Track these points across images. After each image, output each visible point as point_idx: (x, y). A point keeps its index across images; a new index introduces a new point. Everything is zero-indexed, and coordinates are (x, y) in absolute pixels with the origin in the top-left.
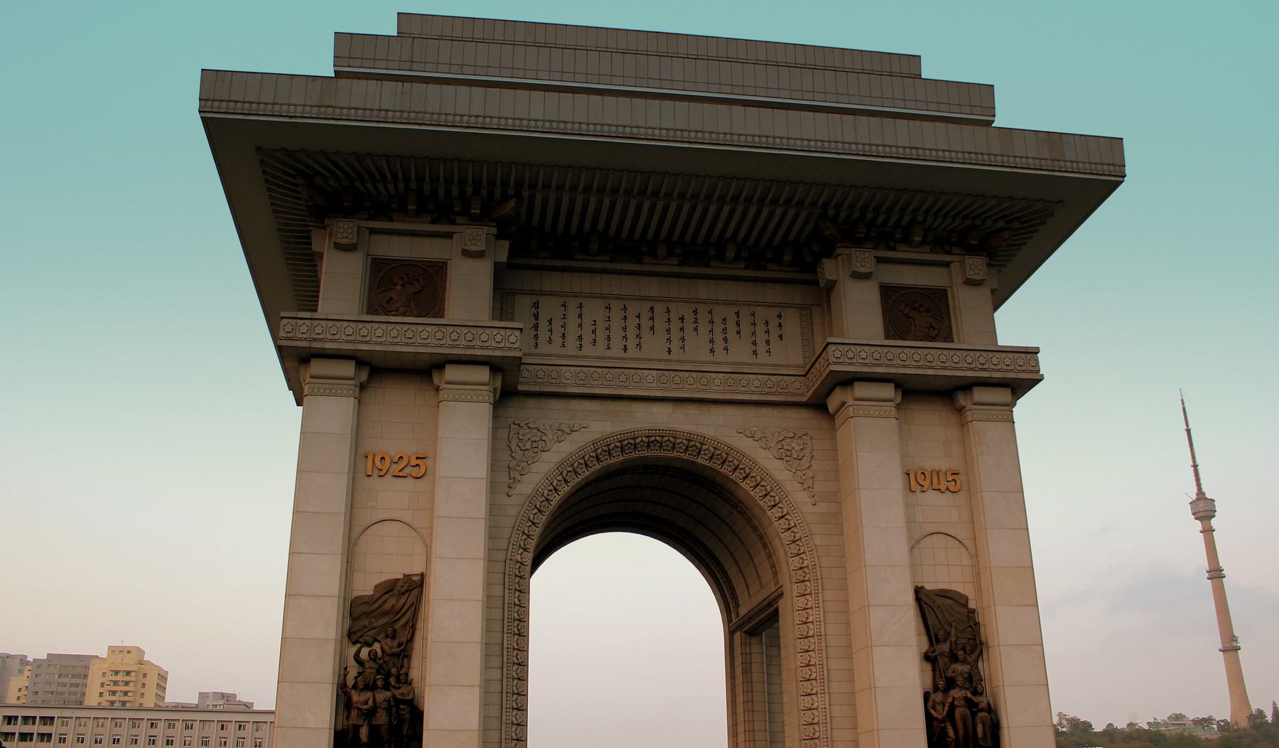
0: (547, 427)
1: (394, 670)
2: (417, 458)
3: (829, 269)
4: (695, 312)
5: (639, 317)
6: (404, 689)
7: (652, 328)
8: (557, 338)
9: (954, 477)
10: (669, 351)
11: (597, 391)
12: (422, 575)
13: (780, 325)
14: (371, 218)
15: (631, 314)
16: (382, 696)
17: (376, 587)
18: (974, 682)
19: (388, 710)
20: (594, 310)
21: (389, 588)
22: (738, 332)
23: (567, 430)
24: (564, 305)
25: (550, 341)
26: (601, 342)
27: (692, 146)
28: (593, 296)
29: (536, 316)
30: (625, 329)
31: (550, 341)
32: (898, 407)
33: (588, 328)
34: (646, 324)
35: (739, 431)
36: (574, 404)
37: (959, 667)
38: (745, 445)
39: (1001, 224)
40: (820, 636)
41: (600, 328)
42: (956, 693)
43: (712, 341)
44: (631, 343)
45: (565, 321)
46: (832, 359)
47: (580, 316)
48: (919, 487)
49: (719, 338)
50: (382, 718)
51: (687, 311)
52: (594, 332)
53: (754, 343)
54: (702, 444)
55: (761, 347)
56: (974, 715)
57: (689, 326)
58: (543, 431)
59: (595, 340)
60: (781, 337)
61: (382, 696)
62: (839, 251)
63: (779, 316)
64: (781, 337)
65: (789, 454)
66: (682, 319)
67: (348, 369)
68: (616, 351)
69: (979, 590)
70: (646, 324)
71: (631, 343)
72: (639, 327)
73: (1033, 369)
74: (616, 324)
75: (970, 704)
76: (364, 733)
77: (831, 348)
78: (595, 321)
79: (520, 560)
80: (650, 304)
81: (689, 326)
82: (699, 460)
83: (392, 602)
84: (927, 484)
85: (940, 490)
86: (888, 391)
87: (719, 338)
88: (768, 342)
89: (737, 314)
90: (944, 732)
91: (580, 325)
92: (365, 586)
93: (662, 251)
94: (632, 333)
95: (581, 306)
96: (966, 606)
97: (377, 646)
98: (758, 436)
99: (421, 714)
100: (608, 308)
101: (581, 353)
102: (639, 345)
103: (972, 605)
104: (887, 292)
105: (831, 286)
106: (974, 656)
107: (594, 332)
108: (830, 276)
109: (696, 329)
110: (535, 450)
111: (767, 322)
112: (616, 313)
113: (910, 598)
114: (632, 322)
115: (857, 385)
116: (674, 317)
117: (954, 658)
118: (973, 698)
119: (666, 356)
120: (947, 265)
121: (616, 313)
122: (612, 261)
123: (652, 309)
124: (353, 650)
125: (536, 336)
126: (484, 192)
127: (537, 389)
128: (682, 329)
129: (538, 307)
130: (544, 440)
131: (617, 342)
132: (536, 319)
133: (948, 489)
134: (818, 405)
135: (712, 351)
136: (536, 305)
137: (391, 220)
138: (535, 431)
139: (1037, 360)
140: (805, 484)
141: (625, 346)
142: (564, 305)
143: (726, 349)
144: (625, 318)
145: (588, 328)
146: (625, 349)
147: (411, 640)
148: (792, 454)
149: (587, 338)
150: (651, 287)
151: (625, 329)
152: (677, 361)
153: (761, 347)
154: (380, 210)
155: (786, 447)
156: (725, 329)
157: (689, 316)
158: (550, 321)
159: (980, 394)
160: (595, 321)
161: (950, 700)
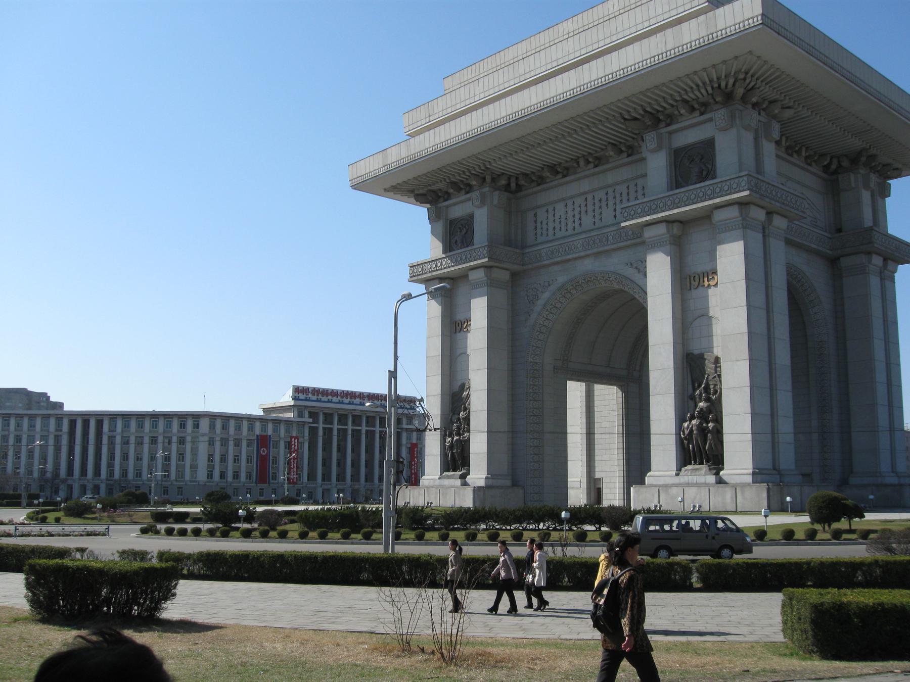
4: (607, 194)
7: (586, 211)
10: (594, 223)
11: (556, 260)
15: (577, 205)
20: (560, 207)
23: (547, 284)
26: (563, 228)
27: (516, 122)
28: (560, 201)
29: (536, 222)
34: (583, 209)
39: (731, 81)
41: (563, 217)
42: (694, 422)
51: (601, 194)
57: (604, 204)
66: (600, 201)
70: (583, 209)
72: (580, 213)
74: (570, 213)
79: (532, 360)
80: (583, 197)
81: (604, 204)
89: (628, 187)
91: (554, 221)
93: (582, 163)
98: (635, 265)
100: (566, 206)
101: (555, 238)
102: (580, 224)
107: (560, 222)
109: (607, 205)
111: (643, 188)
112: (570, 208)
114: (576, 212)
121: (570, 208)
122: (564, 176)
123: (586, 199)
125: (536, 234)
128: (600, 207)
135: (615, 216)
136: (535, 215)
141: (574, 227)
146: (574, 229)
150: (585, 186)
154: (447, 196)
157: (604, 198)
158: (541, 223)
161: (690, 427)
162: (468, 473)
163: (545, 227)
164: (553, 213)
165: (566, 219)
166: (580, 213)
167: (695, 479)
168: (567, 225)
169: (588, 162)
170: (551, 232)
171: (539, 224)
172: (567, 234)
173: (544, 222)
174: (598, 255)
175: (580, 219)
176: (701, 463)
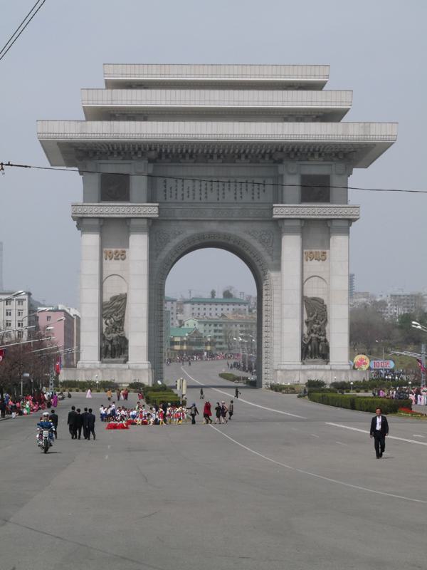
1: (118, 327)
3: (281, 169)
6: (122, 333)
7: (212, 189)
8: (173, 194)
12: (126, 294)
14: (100, 159)
16: (115, 335)
17: (111, 299)
18: (322, 331)
19: (117, 340)
21: (114, 299)
22: (247, 190)
25: (171, 197)
26: (191, 197)
29: (165, 186)
30: (200, 190)
31: (171, 197)
32: (302, 228)
33: (186, 190)
36: (180, 223)
37: (316, 326)
38: (247, 237)
43: (235, 194)
44: (203, 196)
46: (274, 213)
49: (238, 192)
50: (115, 342)
52: (188, 192)
53: (253, 194)
55: (256, 196)
56: (319, 343)
60: (264, 191)
61: (115, 335)
62: (284, 162)
64: (264, 191)
67: (96, 222)
68: (197, 200)
69: (328, 297)
71: (203, 196)
72: (206, 189)
75: (318, 339)
76: (110, 346)
77: (274, 209)
82: (229, 243)
83: (116, 303)
87: (238, 192)
88: (259, 193)
90: (307, 349)
92: (107, 298)
93: (215, 157)
96: (323, 303)
97: (112, 319)
99: (128, 341)
102: (206, 197)
103: (325, 303)
105: (282, 176)
106: (323, 322)
108: (280, 173)
113: (298, 300)
117: (314, 322)
118: (319, 337)
119: (216, 201)
120: (331, 165)
122: (195, 162)
124: (104, 321)
125: (165, 195)
126: (142, 149)
127: (166, 218)
131: (197, 196)
135: (235, 198)
136: (165, 181)
137: (107, 159)
145: (186, 190)
147: (123, 316)
152: (222, 203)
153: (256, 196)
156: (241, 189)
158: (171, 188)
162: (127, 360)
163: (174, 192)
165: (194, 190)
166: (206, 189)
167: (318, 367)
168: (194, 195)
169: (219, 157)
170: (179, 196)
171: (168, 189)
172: (194, 201)
173: (174, 189)
174: (221, 221)
175: (206, 193)
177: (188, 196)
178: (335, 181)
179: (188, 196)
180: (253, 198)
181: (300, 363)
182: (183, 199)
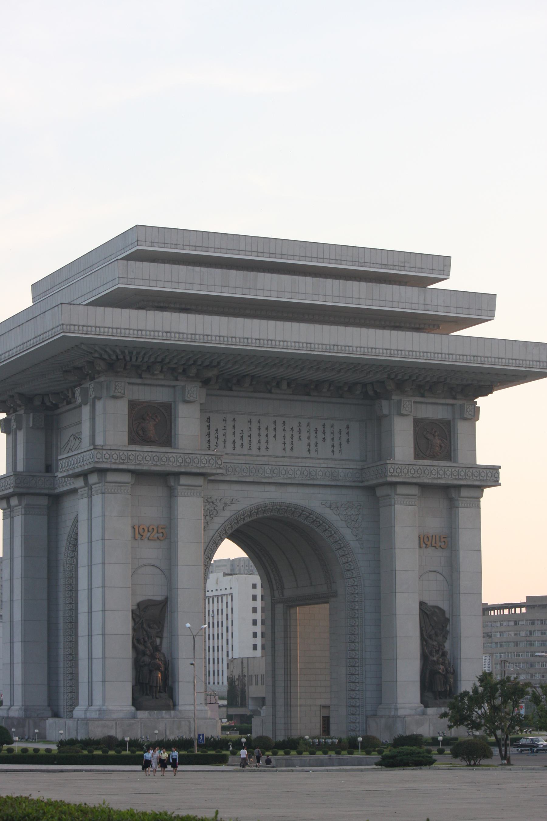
0: (218, 501)
2: (162, 528)
3: (385, 407)
5: (267, 429)
7: (275, 436)
9: (445, 539)
12: (167, 599)
13: (348, 433)
24: (225, 420)
26: (246, 445)
29: (209, 427)
34: (271, 433)
35: (323, 503)
40: (362, 626)
44: (263, 445)
45: (225, 431)
47: (234, 427)
48: (424, 545)
52: (242, 438)
54: (303, 511)
58: (215, 504)
59: (242, 444)
60: (348, 441)
63: (348, 427)
65: (349, 518)
67: (127, 478)
68: (254, 451)
70: (271, 433)
71: (263, 445)
72: (267, 436)
73: (495, 479)
78: (242, 431)
84: (429, 543)
85: (436, 547)
86: (415, 491)
88: (340, 444)
89: (324, 426)
91: (234, 433)
93: (284, 386)
94: (263, 439)
95: (234, 420)
100: (250, 422)
101: (235, 452)
104: (417, 422)
107: (242, 438)
108: (385, 411)
110: (212, 516)
114: (263, 432)
115: (398, 486)
116: (288, 429)
121: (255, 426)
125: (209, 441)
129: (210, 421)
130: (216, 510)
132: (209, 429)
133: (440, 546)
134: (371, 489)
135: (309, 451)
138: (211, 504)
139: (498, 474)
140: (358, 536)
142: (225, 420)
143: (316, 451)
144: (259, 429)
145: (238, 436)
146: (259, 449)
148: (351, 518)
149: (238, 443)
151: (259, 435)
155: (348, 513)
157: (296, 429)
158: (217, 430)
159: (464, 493)
160: (242, 431)
164: (232, 424)
165: (250, 436)
166: (267, 436)
168: (250, 443)
170: (229, 445)
175: (267, 442)
176: (440, 698)
177: (242, 445)
178: (461, 427)
179: (242, 445)
180: (333, 452)
181: (422, 706)
182: (234, 448)
